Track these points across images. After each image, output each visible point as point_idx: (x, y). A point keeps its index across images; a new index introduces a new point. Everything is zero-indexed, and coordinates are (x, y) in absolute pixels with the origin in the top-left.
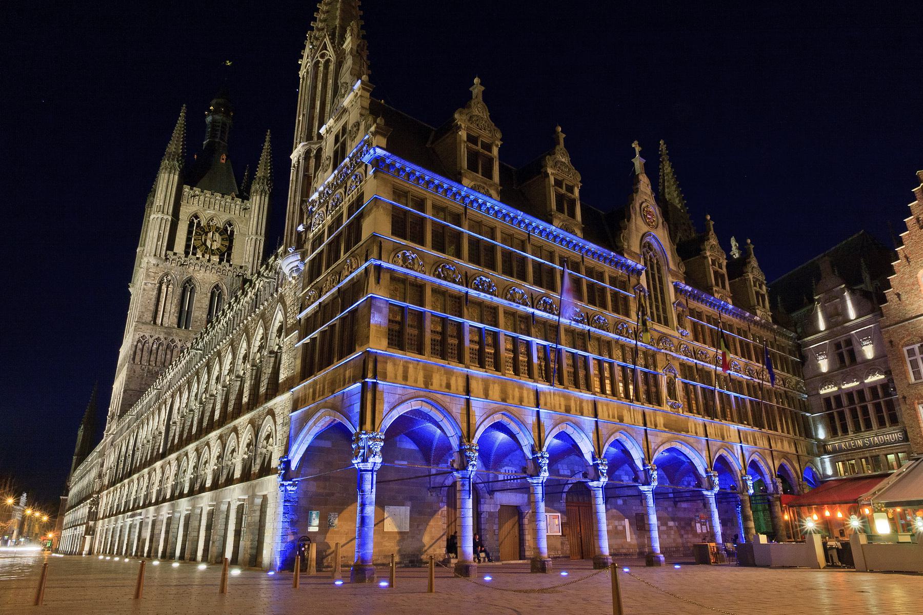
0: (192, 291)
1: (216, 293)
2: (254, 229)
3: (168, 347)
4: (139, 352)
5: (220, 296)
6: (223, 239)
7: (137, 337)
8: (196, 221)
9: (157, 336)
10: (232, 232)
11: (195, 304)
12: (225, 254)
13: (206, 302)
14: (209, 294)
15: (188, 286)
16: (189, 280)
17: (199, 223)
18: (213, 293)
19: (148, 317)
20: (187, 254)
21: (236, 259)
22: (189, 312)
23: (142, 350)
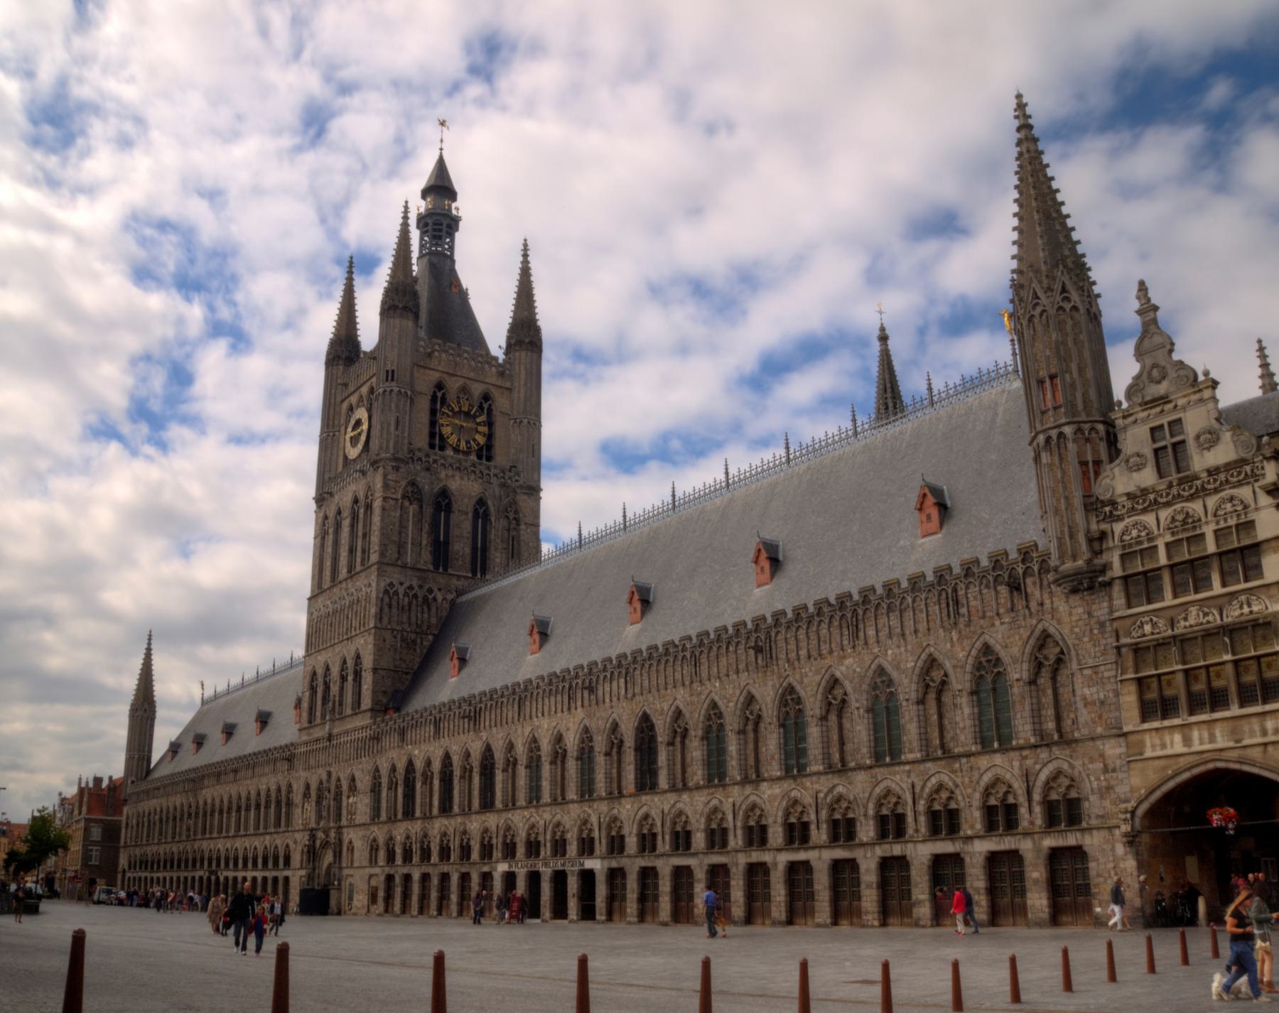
0: (449, 509)
1: (481, 511)
3: (425, 599)
4: (386, 609)
5: (486, 515)
7: (383, 584)
9: (407, 584)
11: (454, 532)
14: (470, 515)
15: (443, 501)
16: (444, 493)
18: (476, 512)
19: (392, 552)
20: (432, 446)
22: (447, 543)
23: (390, 606)
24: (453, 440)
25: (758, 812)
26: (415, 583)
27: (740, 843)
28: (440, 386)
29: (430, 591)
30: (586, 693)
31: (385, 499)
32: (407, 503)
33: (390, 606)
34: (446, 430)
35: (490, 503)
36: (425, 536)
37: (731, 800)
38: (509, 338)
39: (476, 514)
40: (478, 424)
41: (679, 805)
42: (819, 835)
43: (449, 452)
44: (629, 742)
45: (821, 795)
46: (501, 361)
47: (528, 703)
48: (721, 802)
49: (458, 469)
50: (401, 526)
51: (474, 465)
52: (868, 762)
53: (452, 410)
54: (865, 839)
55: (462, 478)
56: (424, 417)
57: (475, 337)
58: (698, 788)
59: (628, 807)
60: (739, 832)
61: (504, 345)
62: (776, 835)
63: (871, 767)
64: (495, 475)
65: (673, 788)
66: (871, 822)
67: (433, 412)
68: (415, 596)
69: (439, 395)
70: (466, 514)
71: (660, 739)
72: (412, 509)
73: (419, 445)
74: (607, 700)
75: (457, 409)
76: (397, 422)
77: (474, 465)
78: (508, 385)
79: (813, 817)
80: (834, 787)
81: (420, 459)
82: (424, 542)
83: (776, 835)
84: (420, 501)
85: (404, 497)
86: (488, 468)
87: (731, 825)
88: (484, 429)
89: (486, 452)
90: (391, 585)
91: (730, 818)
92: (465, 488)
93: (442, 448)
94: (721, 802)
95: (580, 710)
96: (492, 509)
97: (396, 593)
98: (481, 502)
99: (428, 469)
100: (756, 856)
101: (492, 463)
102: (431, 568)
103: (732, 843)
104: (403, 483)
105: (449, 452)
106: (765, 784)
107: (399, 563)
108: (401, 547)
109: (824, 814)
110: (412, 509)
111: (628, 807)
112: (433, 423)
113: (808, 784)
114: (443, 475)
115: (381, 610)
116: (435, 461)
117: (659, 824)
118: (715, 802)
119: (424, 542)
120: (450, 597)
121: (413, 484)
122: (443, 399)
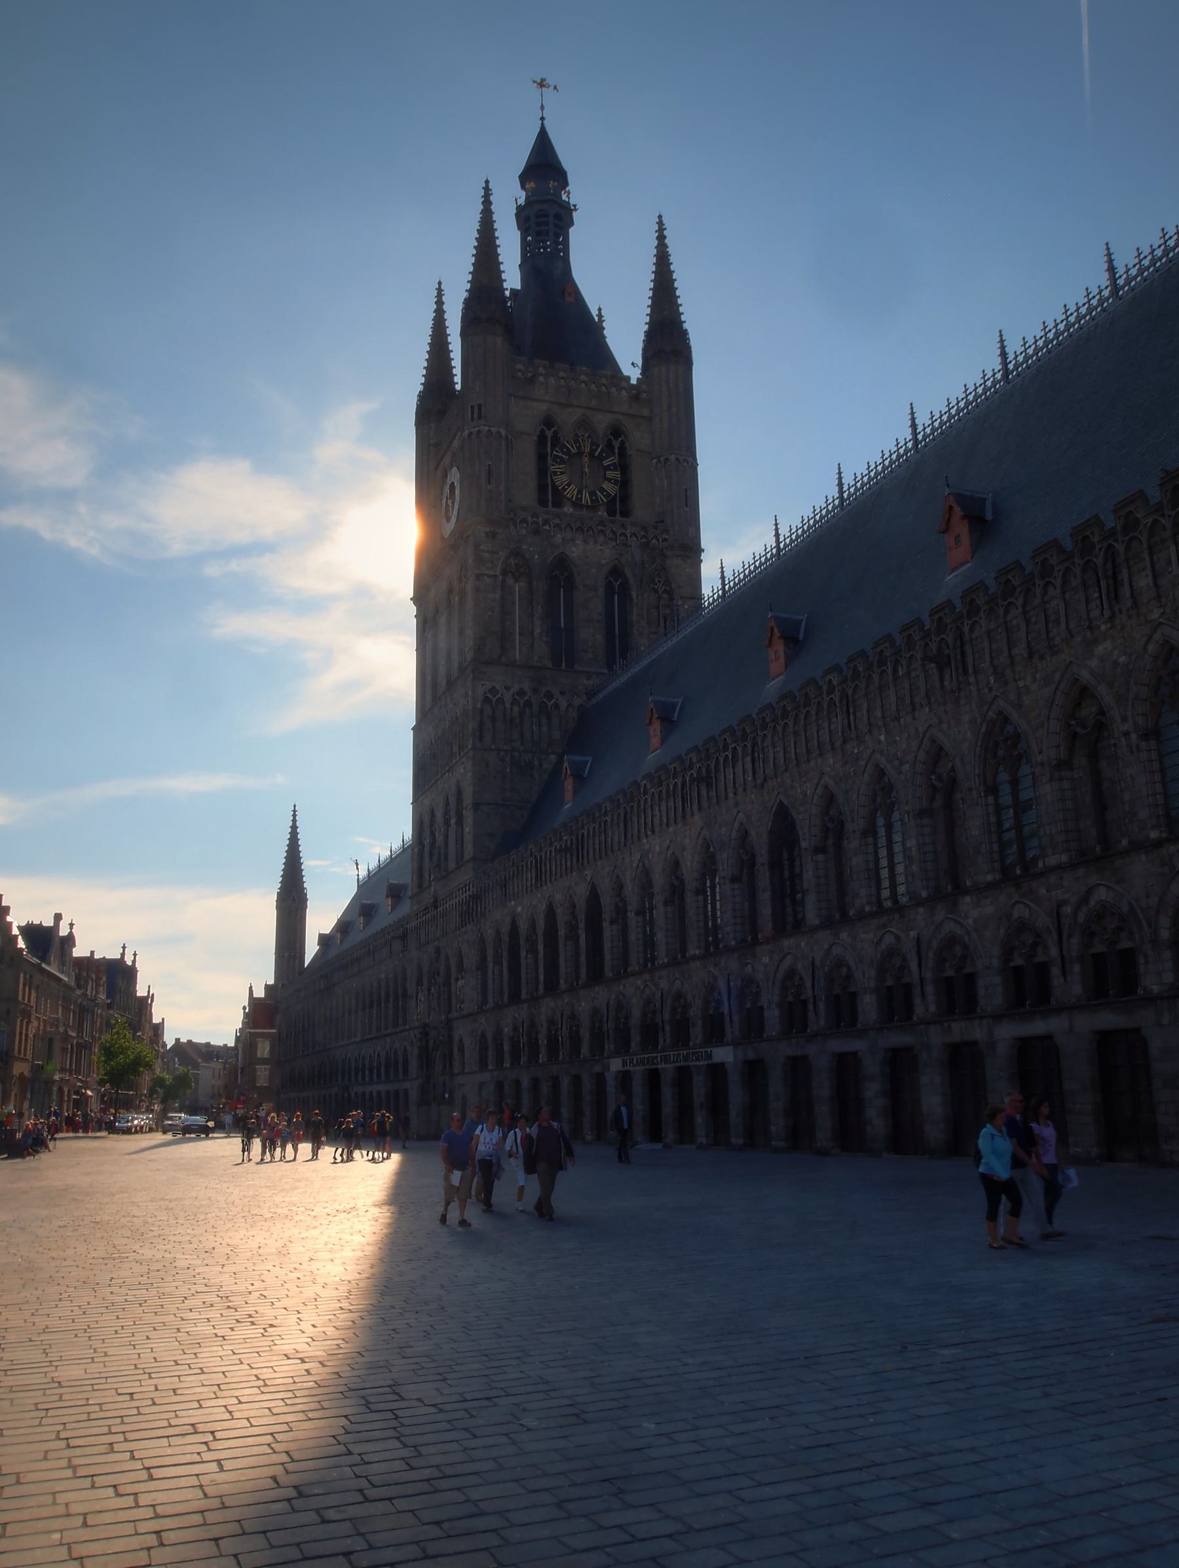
1: (616, 583)
5: (624, 588)
7: (480, 691)
8: (549, 434)
9: (516, 688)
14: (601, 591)
15: (561, 574)
20: (543, 502)
24: (571, 492)
25: (958, 950)
26: (526, 686)
27: (932, 1008)
28: (548, 422)
29: (549, 695)
30: (703, 788)
31: (478, 577)
32: (510, 581)
33: (493, 719)
34: (561, 480)
35: (628, 572)
37: (913, 934)
38: (645, 350)
39: (609, 589)
40: (607, 468)
41: (837, 950)
42: (1069, 985)
43: (568, 509)
44: (763, 857)
45: (1068, 909)
46: (634, 382)
47: (635, 819)
48: (898, 938)
49: (580, 529)
51: (602, 523)
52: (1154, 835)
53: (568, 452)
54: (1155, 989)
55: (586, 542)
56: (529, 465)
57: (602, 358)
58: (862, 916)
59: (766, 960)
60: (930, 989)
61: (640, 362)
62: (992, 990)
63: (1159, 844)
64: (634, 534)
65: (827, 924)
66: (1167, 954)
67: (542, 458)
68: (528, 704)
69: (549, 434)
71: (804, 844)
72: (518, 587)
74: (731, 795)
75: (574, 451)
76: (489, 473)
77: (602, 523)
78: (646, 412)
79: (1054, 952)
80: (1090, 891)
81: (524, 520)
82: (538, 631)
83: (992, 990)
85: (505, 572)
86: (623, 526)
87: (916, 978)
88: (617, 474)
89: (620, 505)
90: (493, 690)
91: (914, 965)
92: (591, 554)
93: (558, 504)
94: (898, 938)
95: (696, 817)
96: (631, 580)
97: (501, 701)
98: (616, 572)
99: (537, 532)
100: (959, 1030)
102: (550, 664)
103: (919, 1010)
105: (568, 509)
106: (968, 899)
107: (504, 659)
109: (1074, 944)
110: (518, 587)
111: (766, 960)
112: (542, 472)
113: (1043, 891)
114: (558, 538)
115: (481, 725)
117: (809, 984)
118: (889, 940)
119: (538, 631)
120: (577, 702)
122: (556, 440)
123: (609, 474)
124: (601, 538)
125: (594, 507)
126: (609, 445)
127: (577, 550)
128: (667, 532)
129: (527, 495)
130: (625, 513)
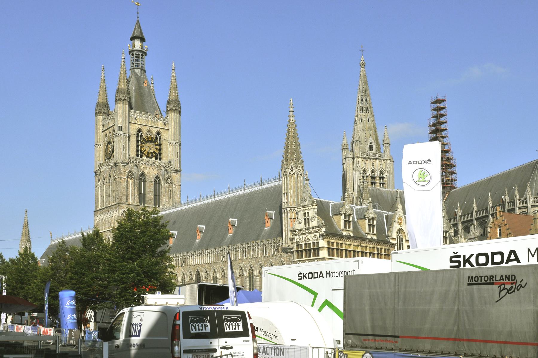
0: (145, 181)
2: (173, 136)
5: (159, 182)
6: (156, 145)
10: (160, 139)
12: (158, 155)
13: (152, 187)
14: (153, 183)
15: (142, 177)
16: (143, 174)
17: (141, 136)
19: (124, 199)
20: (138, 156)
21: (165, 158)
22: (144, 194)
32: (129, 179)
34: (143, 149)
35: (161, 177)
36: (136, 192)
40: (156, 145)
43: (144, 157)
50: (127, 189)
70: (152, 182)
73: (133, 156)
77: (154, 163)
81: (133, 162)
84: (134, 178)
85: (128, 177)
92: (151, 172)
93: (141, 156)
96: (162, 180)
98: (157, 177)
101: (162, 161)
104: (127, 172)
105: (144, 157)
108: (127, 196)
110: (130, 181)
112: (138, 146)
114: (142, 168)
116: (139, 162)
121: (130, 172)
123: (157, 147)
124: (154, 167)
125: (151, 158)
126: (156, 138)
127: (146, 171)
128: (172, 165)
129: (133, 154)
130: (160, 159)
